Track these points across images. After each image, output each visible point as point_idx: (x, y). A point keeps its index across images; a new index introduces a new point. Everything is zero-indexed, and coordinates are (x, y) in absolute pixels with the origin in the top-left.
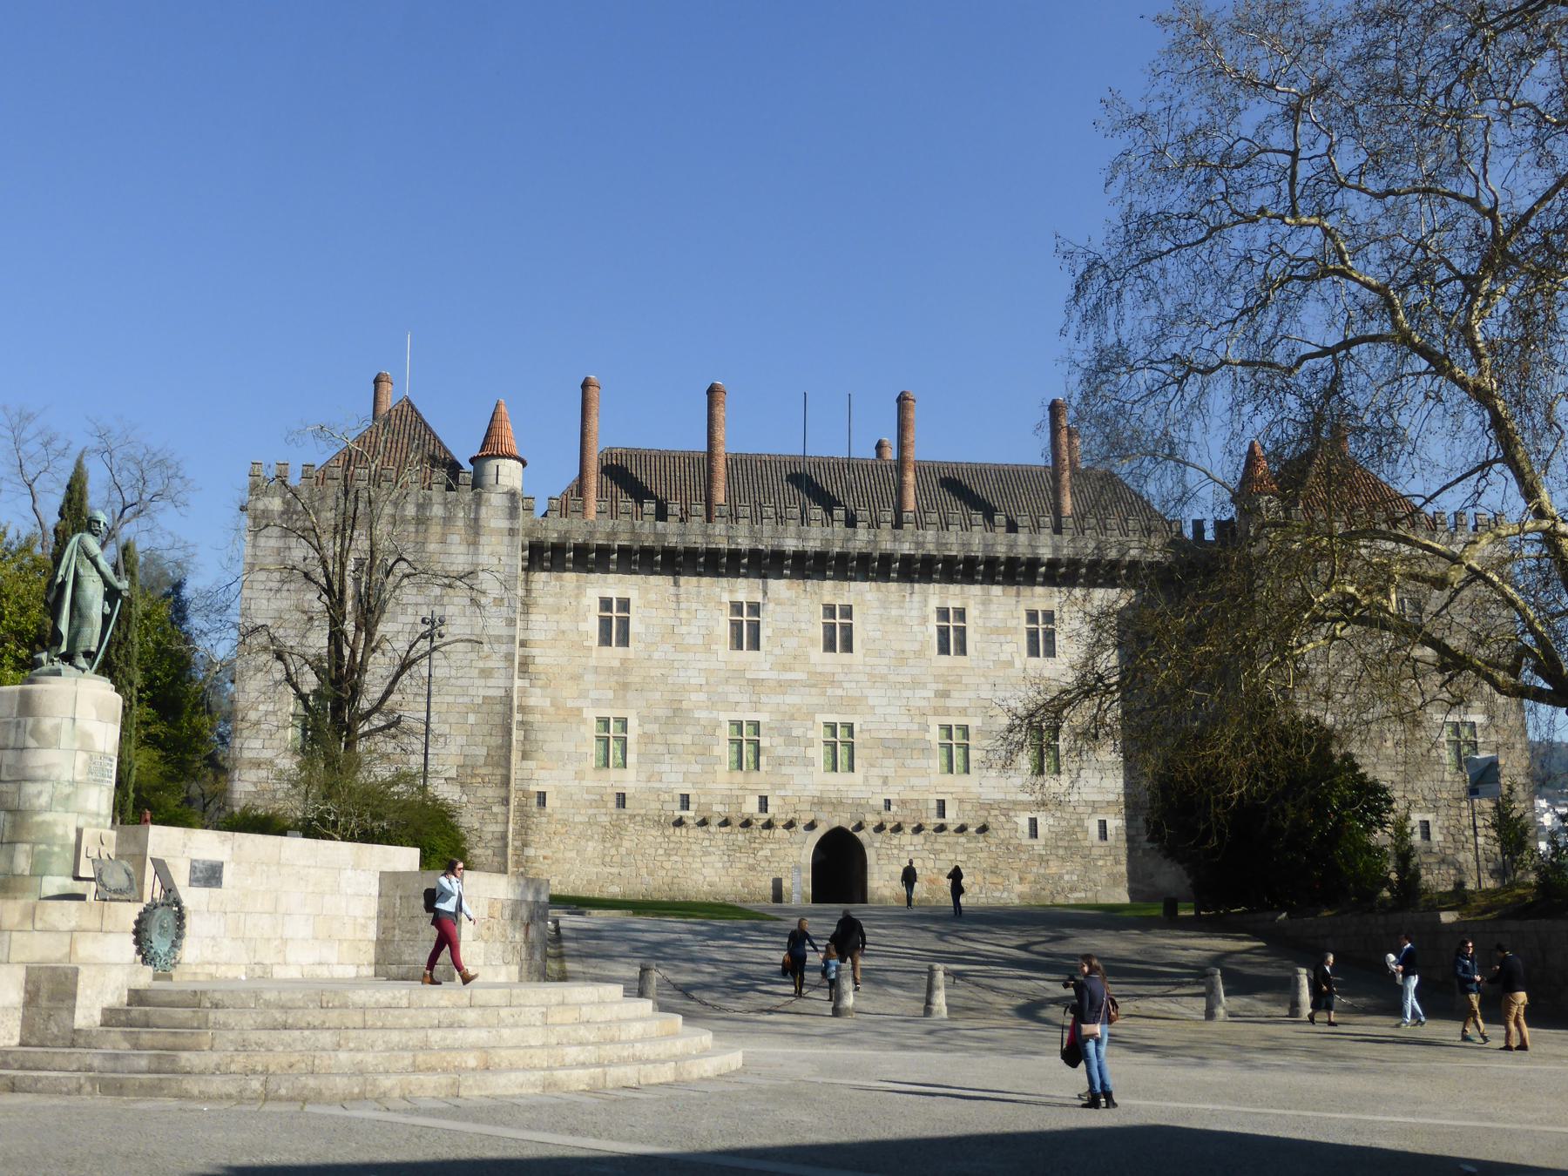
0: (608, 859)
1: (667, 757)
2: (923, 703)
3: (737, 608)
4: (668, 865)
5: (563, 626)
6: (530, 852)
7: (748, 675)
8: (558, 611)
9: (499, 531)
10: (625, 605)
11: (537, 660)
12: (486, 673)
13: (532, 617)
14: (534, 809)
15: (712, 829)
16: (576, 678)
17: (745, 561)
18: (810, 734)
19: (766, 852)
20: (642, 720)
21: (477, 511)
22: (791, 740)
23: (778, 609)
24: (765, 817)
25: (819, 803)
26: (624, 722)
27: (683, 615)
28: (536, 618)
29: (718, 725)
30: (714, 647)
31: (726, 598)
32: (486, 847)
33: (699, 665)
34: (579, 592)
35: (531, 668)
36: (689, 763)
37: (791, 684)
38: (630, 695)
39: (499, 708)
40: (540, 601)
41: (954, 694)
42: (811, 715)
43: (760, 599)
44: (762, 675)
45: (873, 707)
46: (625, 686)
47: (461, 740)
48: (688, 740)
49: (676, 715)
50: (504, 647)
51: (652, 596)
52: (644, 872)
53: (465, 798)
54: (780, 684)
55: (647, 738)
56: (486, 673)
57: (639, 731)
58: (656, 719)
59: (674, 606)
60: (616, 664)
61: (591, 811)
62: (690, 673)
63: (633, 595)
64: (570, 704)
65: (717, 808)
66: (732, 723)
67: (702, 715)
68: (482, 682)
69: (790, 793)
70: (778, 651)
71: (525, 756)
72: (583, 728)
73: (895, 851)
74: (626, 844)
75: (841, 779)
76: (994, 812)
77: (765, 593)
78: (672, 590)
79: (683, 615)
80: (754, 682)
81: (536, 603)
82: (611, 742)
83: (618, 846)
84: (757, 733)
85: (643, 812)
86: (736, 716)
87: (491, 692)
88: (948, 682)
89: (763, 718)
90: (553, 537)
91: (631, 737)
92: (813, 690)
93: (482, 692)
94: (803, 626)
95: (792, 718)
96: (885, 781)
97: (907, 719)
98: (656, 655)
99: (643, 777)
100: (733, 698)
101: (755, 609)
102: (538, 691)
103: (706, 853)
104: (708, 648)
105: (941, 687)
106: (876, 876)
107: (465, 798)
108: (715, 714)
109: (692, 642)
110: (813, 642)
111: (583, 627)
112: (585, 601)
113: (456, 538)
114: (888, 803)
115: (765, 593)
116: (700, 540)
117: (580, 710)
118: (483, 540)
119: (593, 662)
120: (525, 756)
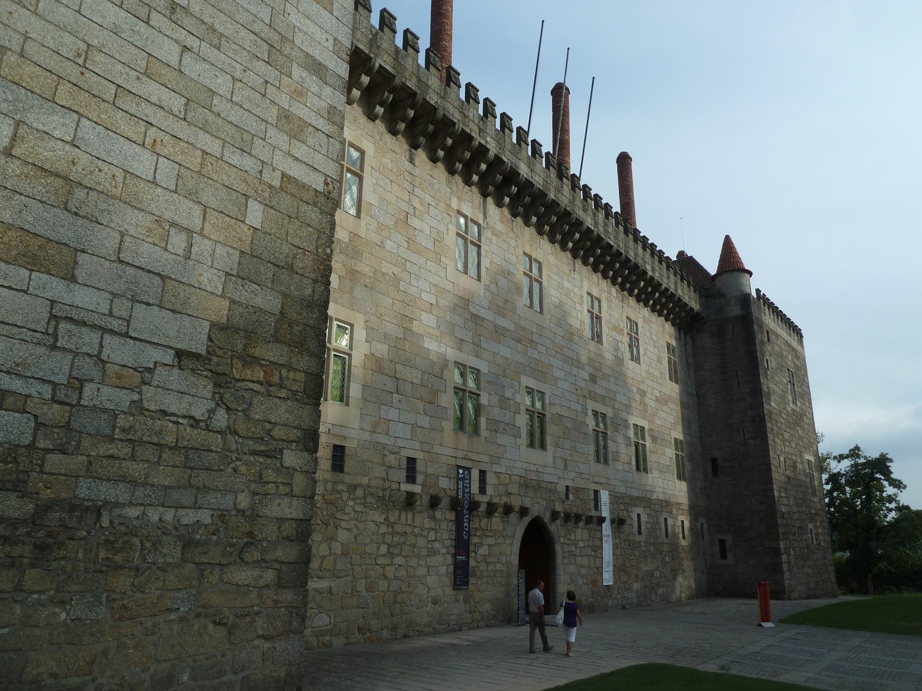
2: (583, 385)
4: (390, 571)
15: (438, 515)
18: (518, 398)
24: (484, 499)
25: (527, 485)
30: (443, 259)
33: (431, 281)
38: (359, 291)
41: (599, 381)
44: (484, 313)
45: (556, 379)
52: (361, 585)
53: (221, 419)
58: (386, 336)
59: (409, 187)
62: (421, 283)
63: (369, 148)
65: (445, 483)
68: (280, 140)
73: (573, 548)
74: (343, 535)
75: (535, 455)
76: (622, 507)
78: (407, 165)
79: (416, 203)
83: (333, 538)
85: (365, 481)
87: (297, 172)
88: (594, 367)
89: (484, 367)
96: (565, 466)
97: (574, 398)
98: (389, 245)
103: (432, 552)
105: (591, 370)
106: (562, 578)
107: (221, 419)
114: (567, 487)
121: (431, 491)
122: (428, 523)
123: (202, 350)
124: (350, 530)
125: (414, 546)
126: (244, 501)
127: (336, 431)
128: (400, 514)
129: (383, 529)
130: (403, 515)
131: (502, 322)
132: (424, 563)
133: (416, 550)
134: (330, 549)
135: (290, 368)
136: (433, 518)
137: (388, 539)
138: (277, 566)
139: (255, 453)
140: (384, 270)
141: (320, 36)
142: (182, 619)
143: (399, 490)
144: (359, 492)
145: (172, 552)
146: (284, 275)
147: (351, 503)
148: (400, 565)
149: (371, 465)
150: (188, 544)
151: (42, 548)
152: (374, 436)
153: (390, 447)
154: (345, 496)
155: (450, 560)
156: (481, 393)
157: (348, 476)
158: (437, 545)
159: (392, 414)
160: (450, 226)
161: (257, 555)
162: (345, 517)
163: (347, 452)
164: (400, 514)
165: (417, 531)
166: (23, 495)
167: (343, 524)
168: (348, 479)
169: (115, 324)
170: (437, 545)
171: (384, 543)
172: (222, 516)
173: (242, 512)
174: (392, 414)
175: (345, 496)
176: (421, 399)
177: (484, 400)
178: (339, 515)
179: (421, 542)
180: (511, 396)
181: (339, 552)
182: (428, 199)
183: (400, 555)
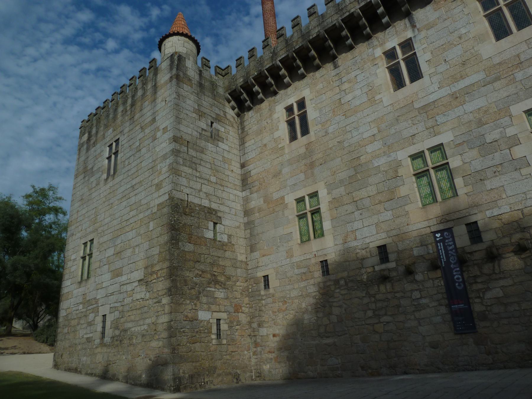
0: (322, 330)
1: (357, 213)
3: (391, 55)
5: (265, 142)
6: (263, 331)
7: (417, 105)
8: (260, 132)
9: (166, 83)
10: (301, 104)
11: (253, 173)
12: (159, 186)
13: (247, 145)
14: (263, 292)
15: (419, 277)
16: (277, 175)
17: (381, 10)
18: (510, 132)
19: (496, 292)
20: (330, 187)
21: (155, 80)
22: (487, 149)
23: (431, 32)
26: (314, 195)
27: (346, 86)
28: (250, 143)
29: (399, 164)
31: (379, 52)
32: (158, 339)
33: (369, 120)
34: (271, 111)
35: (250, 180)
36: (379, 212)
37: (468, 91)
39: (165, 210)
40: (250, 131)
42: (504, 111)
43: (409, 34)
46: (312, 165)
47: (146, 246)
48: (372, 190)
49: (358, 172)
50: (168, 160)
51: (320, 86)
54: (454, 96)
55: (336, 203)
56: (159, 186)
57: (328, 198)
58: (341, 181)
59: (338, 83)
60: (303, 150)
61: (303, 284)
64: (276, 196)
66: (414, 157)
67: (381, 162)
69: (506, 209)
70: (442, 68)
71: (252, 248)
72: (286, 212)
74: (336, 311)
77: (413, 26)
78: (334, 73)
80: (425, 109)
81: (247, 134)
82: (310, 217)
84: (444, 156)
85: (345, 274)
86: (414, 150)
89: (445, 138)
90: (240, 81)
91: (324, 207)
92: (497, 85)
93: (157, 202)
94: (463, 31)
95: (480, 123)
98: (331, 130)
99: (340, 241)
100: (406, 134)
101: (407, 45)
102: (255, 195)
104: (372, 101)
108: (393, 155)
109: (358, 103)
110: (480, 38)
111: (276, 135)
112: (275, 116)
113: (147, 103)
115: (413, 26)
116: (336, 17)
117: (283, 198)
118: (159, 93)
119: (287, 157)
120: (252, 248)
121: (407, 262)
122: (408, 287)
123: (143, 277)
124: (340, 306)
125: (399, 306)
126: (154, 319)
127: (320, 253)
128: (378, 287)
129: (366, 301)
130: (382, 288)
131: (462, 84)
132: (413, 317)
133: (400, 309)
134: (329, 320)
135: (161, 269)
136: (415, 281)
137: (373, 306)
138: (162, 340)
139: (155, 303)
140: (330, 146)
141: (164, 145)
142: (143, 358)
143: (374, 271)
144: (342, 282)
145: (140, 338)
146: (159, 239)
147: (337, 291)
148: (388, 322)
149: (347, 263)
150: (143, 336)
151: (121, 341)
152: (346, 245)
153: (360, 247)
154: (333, 288)
155: (444, 310)
156: (449, 160)
157: (332, 276)
158: (424, 301)
159: (357, 225)
160: (378, 71)
161: (157, 337)
162: (335, 300)
163: (329, 262)
164: (378, 287)
165: (398, 295)
166: (119, 329)
167: (335, 304)
168: (332, 277)
169: (128, 281)
170: (424, 301)
171: (370, 309)
172: (149, 325)
173: (153, 323)
174: (357, 225)
175: (333, 288)
176: (380, 202)
177: (454, 163)
178: (331, 300)
179: (403, 302)
180: (497, 137)
181: (336, 321)
182: (353, 74)
183: (386, 314)
